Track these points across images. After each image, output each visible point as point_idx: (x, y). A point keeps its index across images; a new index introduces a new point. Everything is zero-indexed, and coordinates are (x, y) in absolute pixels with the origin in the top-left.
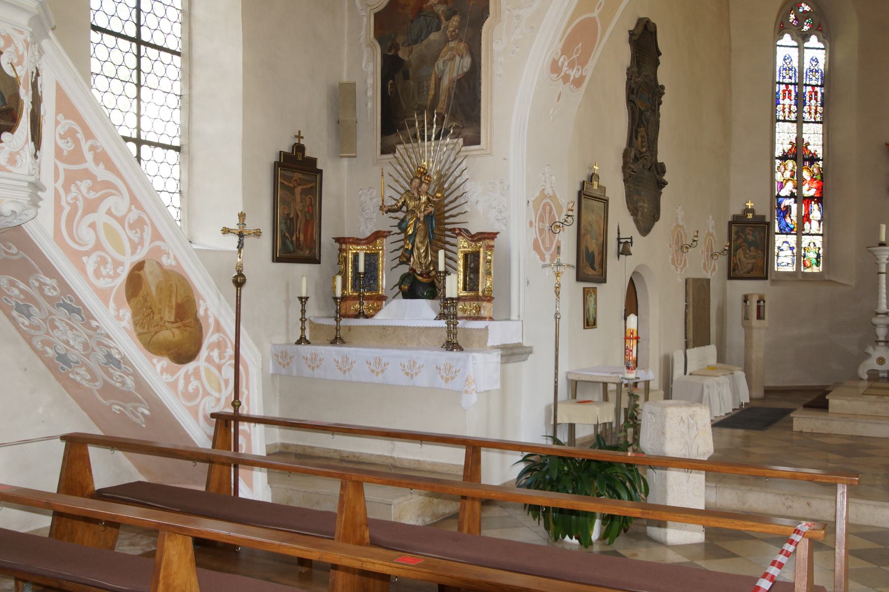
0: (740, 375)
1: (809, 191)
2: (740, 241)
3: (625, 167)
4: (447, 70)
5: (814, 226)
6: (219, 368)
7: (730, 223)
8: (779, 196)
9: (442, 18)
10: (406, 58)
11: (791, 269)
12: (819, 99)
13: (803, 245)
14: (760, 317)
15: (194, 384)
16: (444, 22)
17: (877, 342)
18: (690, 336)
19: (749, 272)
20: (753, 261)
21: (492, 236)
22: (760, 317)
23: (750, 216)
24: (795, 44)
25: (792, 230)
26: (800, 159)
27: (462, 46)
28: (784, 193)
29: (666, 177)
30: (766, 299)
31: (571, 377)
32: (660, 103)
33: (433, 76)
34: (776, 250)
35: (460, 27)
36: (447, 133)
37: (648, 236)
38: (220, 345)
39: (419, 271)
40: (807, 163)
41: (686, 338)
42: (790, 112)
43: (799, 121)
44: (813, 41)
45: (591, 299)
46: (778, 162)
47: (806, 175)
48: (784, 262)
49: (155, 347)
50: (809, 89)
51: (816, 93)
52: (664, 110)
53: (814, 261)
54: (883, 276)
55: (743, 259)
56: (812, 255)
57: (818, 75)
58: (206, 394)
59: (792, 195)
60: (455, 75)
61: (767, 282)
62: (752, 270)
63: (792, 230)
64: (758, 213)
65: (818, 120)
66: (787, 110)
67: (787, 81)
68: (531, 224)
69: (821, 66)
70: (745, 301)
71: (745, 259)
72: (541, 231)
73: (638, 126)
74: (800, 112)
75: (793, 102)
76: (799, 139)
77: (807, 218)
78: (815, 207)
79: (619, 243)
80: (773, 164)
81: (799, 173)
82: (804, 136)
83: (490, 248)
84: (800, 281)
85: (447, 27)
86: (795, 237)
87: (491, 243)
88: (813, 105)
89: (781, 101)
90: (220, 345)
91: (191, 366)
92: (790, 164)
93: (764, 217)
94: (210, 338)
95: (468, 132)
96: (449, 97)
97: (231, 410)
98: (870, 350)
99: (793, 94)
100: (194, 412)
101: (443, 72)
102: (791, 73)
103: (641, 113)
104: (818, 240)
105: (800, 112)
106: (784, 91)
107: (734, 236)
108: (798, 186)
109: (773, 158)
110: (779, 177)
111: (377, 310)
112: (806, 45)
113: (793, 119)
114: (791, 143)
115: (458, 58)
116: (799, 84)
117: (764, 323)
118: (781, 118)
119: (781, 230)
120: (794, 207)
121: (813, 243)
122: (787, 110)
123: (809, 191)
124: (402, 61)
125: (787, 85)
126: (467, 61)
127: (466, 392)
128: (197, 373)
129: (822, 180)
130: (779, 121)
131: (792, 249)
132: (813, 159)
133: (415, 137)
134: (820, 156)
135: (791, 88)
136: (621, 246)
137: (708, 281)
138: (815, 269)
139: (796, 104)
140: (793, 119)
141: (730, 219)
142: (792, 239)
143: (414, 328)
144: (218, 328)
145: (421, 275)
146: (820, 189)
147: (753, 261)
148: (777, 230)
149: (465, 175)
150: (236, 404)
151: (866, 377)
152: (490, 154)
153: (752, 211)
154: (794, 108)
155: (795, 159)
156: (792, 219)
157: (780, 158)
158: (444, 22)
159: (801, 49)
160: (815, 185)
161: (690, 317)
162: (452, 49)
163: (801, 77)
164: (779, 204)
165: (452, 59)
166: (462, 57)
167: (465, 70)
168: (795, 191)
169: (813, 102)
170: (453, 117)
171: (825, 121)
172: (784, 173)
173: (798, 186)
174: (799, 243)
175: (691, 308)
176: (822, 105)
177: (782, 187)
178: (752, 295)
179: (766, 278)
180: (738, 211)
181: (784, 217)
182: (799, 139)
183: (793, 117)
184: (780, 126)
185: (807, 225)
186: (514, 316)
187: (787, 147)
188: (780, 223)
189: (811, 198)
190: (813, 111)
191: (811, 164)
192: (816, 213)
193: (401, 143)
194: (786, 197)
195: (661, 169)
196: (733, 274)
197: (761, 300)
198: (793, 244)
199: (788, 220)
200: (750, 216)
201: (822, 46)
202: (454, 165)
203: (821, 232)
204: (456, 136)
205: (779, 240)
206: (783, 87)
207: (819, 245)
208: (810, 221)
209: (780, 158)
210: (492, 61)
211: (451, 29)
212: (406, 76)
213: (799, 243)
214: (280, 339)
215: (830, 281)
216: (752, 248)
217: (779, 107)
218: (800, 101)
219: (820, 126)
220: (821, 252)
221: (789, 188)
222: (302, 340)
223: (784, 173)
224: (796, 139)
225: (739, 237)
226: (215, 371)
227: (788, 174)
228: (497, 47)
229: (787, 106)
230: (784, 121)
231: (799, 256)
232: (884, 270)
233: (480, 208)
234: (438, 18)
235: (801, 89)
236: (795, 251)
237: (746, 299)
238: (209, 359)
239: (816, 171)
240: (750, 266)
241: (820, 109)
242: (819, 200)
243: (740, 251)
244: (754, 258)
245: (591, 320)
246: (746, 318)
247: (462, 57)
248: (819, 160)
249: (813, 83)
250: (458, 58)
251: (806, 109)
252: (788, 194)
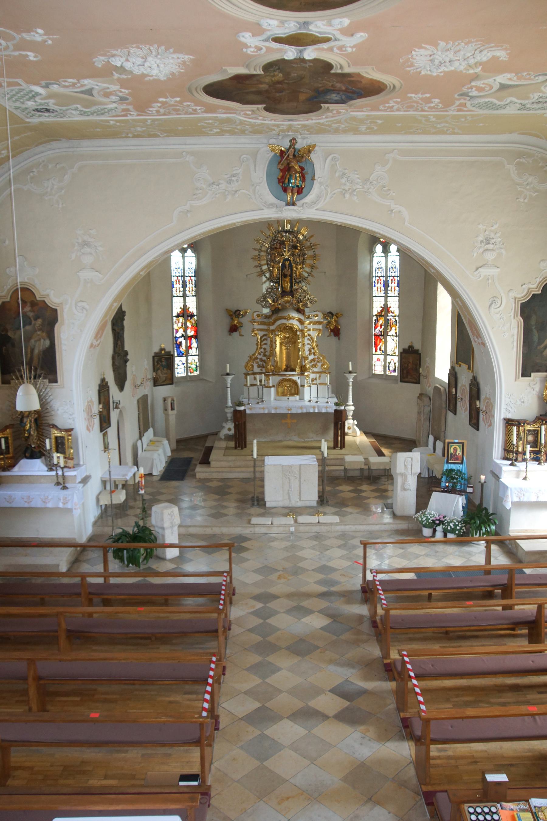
0: (166, 442)
1: (191, 333)
2: (159, 366)
3: (114, 364)
4: (37, 345)
5: (194, 351)
7: (154, 357)
8: (176, 337)
9: (32, 319)
10: (12, 337)
11: (184, 375)
12: (193, 283)
13: (189, 362)
14: (172, 409)
16: (33, 321)
17: (228, 420)
18: (142, 428)
19: (164, 382)
20: (166, 375)
21: (72, 430)
22: (172, 409)
23: (163, 352)
24: (181, 254)
25: (183, 354)
26: (186, 316)
27: (44, 334)
28: (179, 335)
29: (128, 357)
30: (175, 399)
31: (103, 479)
32: (124, 320)
33: (29, 348)
34: (176, 366)
35: (42, 324)
36: (40, 376)
37: (123, 392)
39: (33, 446)
40: (189, 318)
41: (139, 429)
42: (180, 291)
43: (184, 296)
44: (189, 251)
45: (106, 437)
46: (175, 319)
47: (189, 324)
48: (180, 371)
50: (188, 278)
51: (192, 280)
52: (125, 323)
53: (195, 369)
54: (229, 389)
55: (161, 375)
56: (194, 366)
57: (193, 271)
59: (183, 336)
60: (41, 348)
61: (173, 386)
62: (165, 380)
63: (183, 354)
64: (167, 350)
65: (194, 294)
66: (178, 291)
67: (177, 275)
68: (85, 419)
69: (194, 266)
70: (164, 401)
71: (162, 375)
72: (88, 420)
73: (117, 341)
74: (184, 291)
75: (181, 286)
76: (185, 306)
77: (190, 347)
78: (194, 340)
79: (114, 403)
80: (172, 320)
81: (186, 324)
82: (187, 304)
83: (70, 435)
84: (188, 381)
85: (35, 324)
86: (185, 358)
87: (70, 433)
88: (191, 287)
89: (175, 286)
92: (181, 319)
93: (170, 352)
95: (51, 377)
96: (39, 359)
98: (224, 424)
99: (181, 282)
101: (35, 346)
102: (179, 270)
103: (118, 333)
104: (196, 358)
105: (184, 291)
106: (176, 281)
107: (156, 364)
108: (185, 331)
109: (172, 317)
110: (175, 327)
111: (13, 466)
112: (186, 254)
113: (182, 295)
114: (181, 308)
115: (42, 340)
116: (184, 276)
117: (175, 412)
118: (175, 295)
119: (178, 354)
120: (184, 342)
121: (194, 360)
122: (178, 291)
123: (191, 333)
124: (10, 338)
125: (177, 277)
126: (47, 343)
127: (75, 509)
129: (196, 327)
130: (174, 296)
131: (183, 364)
132: (192, 316)
133: (21, 376)
134: (195, 314)
135: (180, 278)
136: (115, 404)
137: (147, 395)
138: (196, 373)
139: (183, 287)
140: (182, 295)
141: (153, 355)
142: (183, 359)
143: (37, 476)
145: (35, 448)
146: (196, 332)
147: (166, 375)
148: (176, 355)
149: (51, 397)
151: (223, 437)
152: (63, 387)
153: (164, 349)
154: (182, 289)
155: (183, 316)
156: (183, 349)
157: (176, 317)
158: (33, 321)
159: (183, 257)
160: (193, 329)
161: (141, 419)
162: (39, 335)
163: (184, 273)
164: (176, 341)
165: (39, 340)
166: (45, 340)
167: (47, 346)
168: (184, 333)
169: (191, 285)
170: (42, 369)
171: (197, 295)
172: (178, 325)
173: (185, 331)
174: (187, 360)
175: (141, 415)
176: (195, 287)
177: (177, 331)
178: (168, 397)
179: (172, 384)
180: (156, 350)
181: (179, 348)
182: (185, 306)
183: (181, 294)
184: (174, 298)
185: (190, 351)
187: (179, 310)
188: (177, 351)
189: (192, 337)
190: (191, 290)
191: (191, 318)
192: (194, 344)
193: (13, 379)
194: (180, 337)
195: (126, 353)
196: (156, 383)
197: (173, 400)
198: (184, 362)
199: (181, 349)
200: (163, 352)
201: (194, 255)
202: (46, 393)
203: (197, 354)
204: (45, 378)
205: (177, 360)
206: (176, 278)
207: (197, 360)
208: (191, 348)
209: (176, 317)
210: (61, 344)
211: (38, 325)
212: (13, 345)
213: (187, 360)
215: (203, 379)
216: (165, 369)
217: (174, 289)
218: (184, 285)
219: (195, 297)
220: (198, 364)
221: (181, 332)
223: (178, 325)
224: (184, 306)
225: (158, 363)
227: (180, 325)
228: (62, 336)
229: (178, 288)
230: (177, 296)
231: (187, 368)
232: (229, 386)
233: (59, 412)
234: (30, 318)
235: (184, 278)
236: (185, 365)
237: (165, 400)
239: (193, 322)
240: (164, 378)
241: (194, 289)
242: (196, 337)
243: (159, 372)
244: (166, 374)
246: (166, 410)
247: (45, 340)
248: (194, 316)
249: (190, 275)
250: (42, 340)
251: (187, 289)
252: (180, 335)
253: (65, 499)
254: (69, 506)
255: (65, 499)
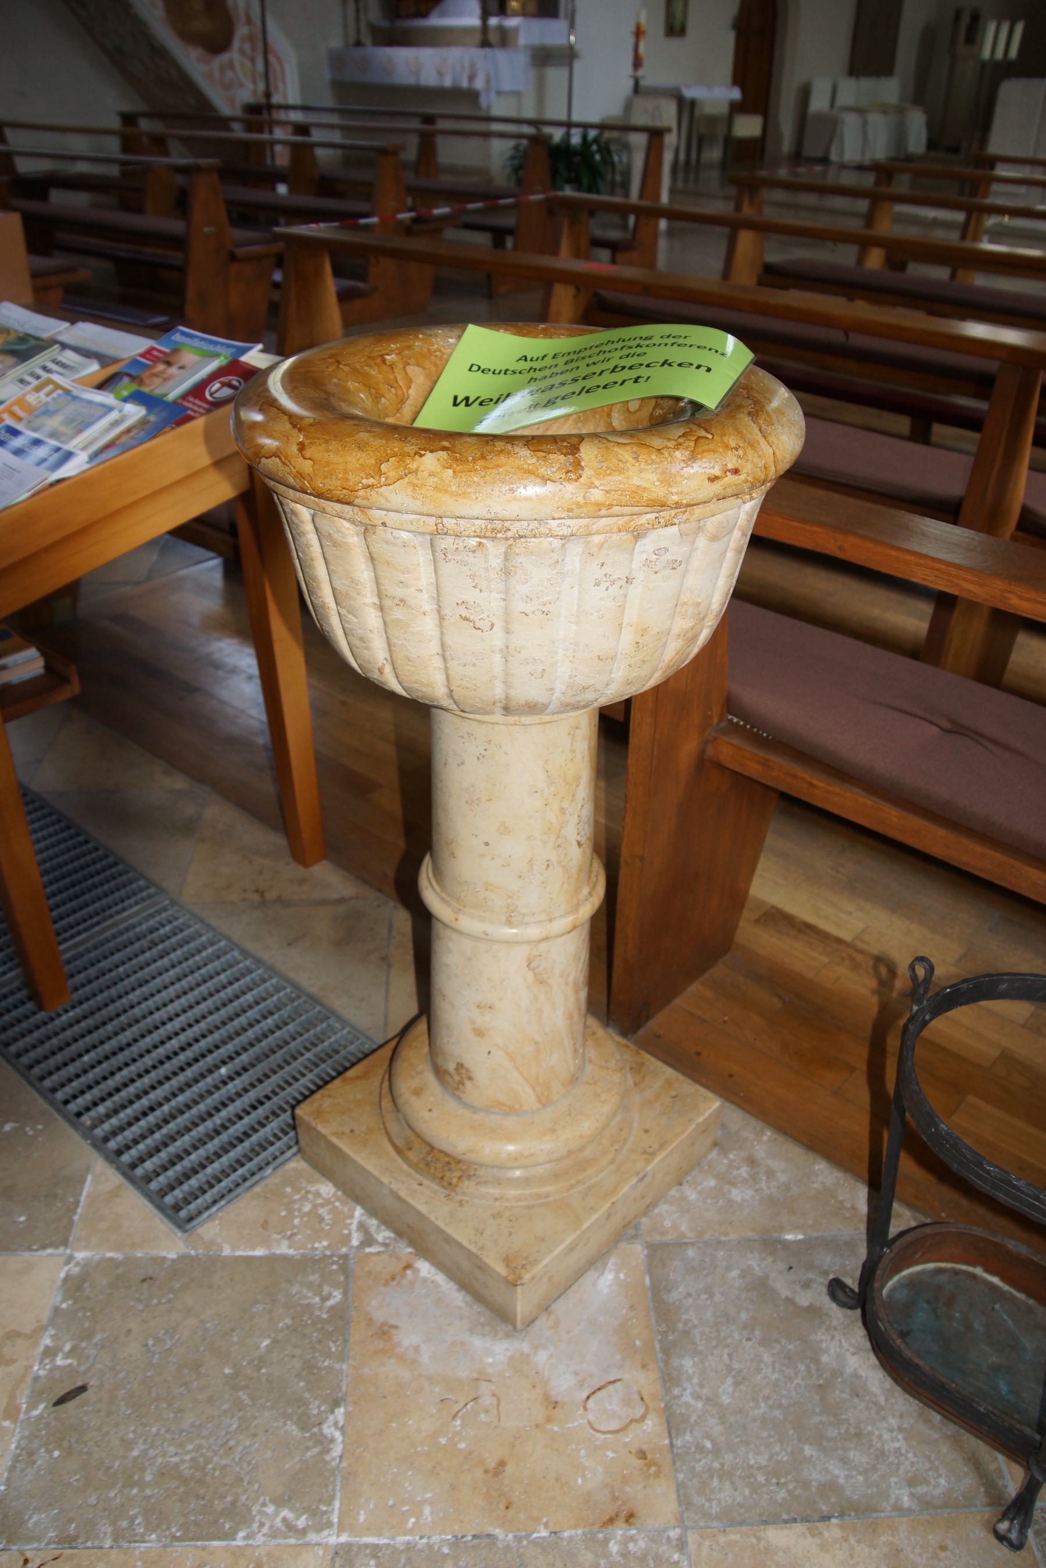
6: (253, 60)
15: (229, 74)
38: (251, 38)
49: (189, 37)
58: (241, 85)
90: (251, 38)
91: (224, 57)
94: (241, 31)
97: (263, 101)
100: (232, 101)
128: (231, 65)
144: (249, 21)
150: (268, 95)
186: (562, 13)
214: (336, 43)
222: (358, 43)
226: (248, 63)
238: (242, 52)
245: (677, 25)
253: (473, 65)
254: (479, 84)
255: (473, 65)
